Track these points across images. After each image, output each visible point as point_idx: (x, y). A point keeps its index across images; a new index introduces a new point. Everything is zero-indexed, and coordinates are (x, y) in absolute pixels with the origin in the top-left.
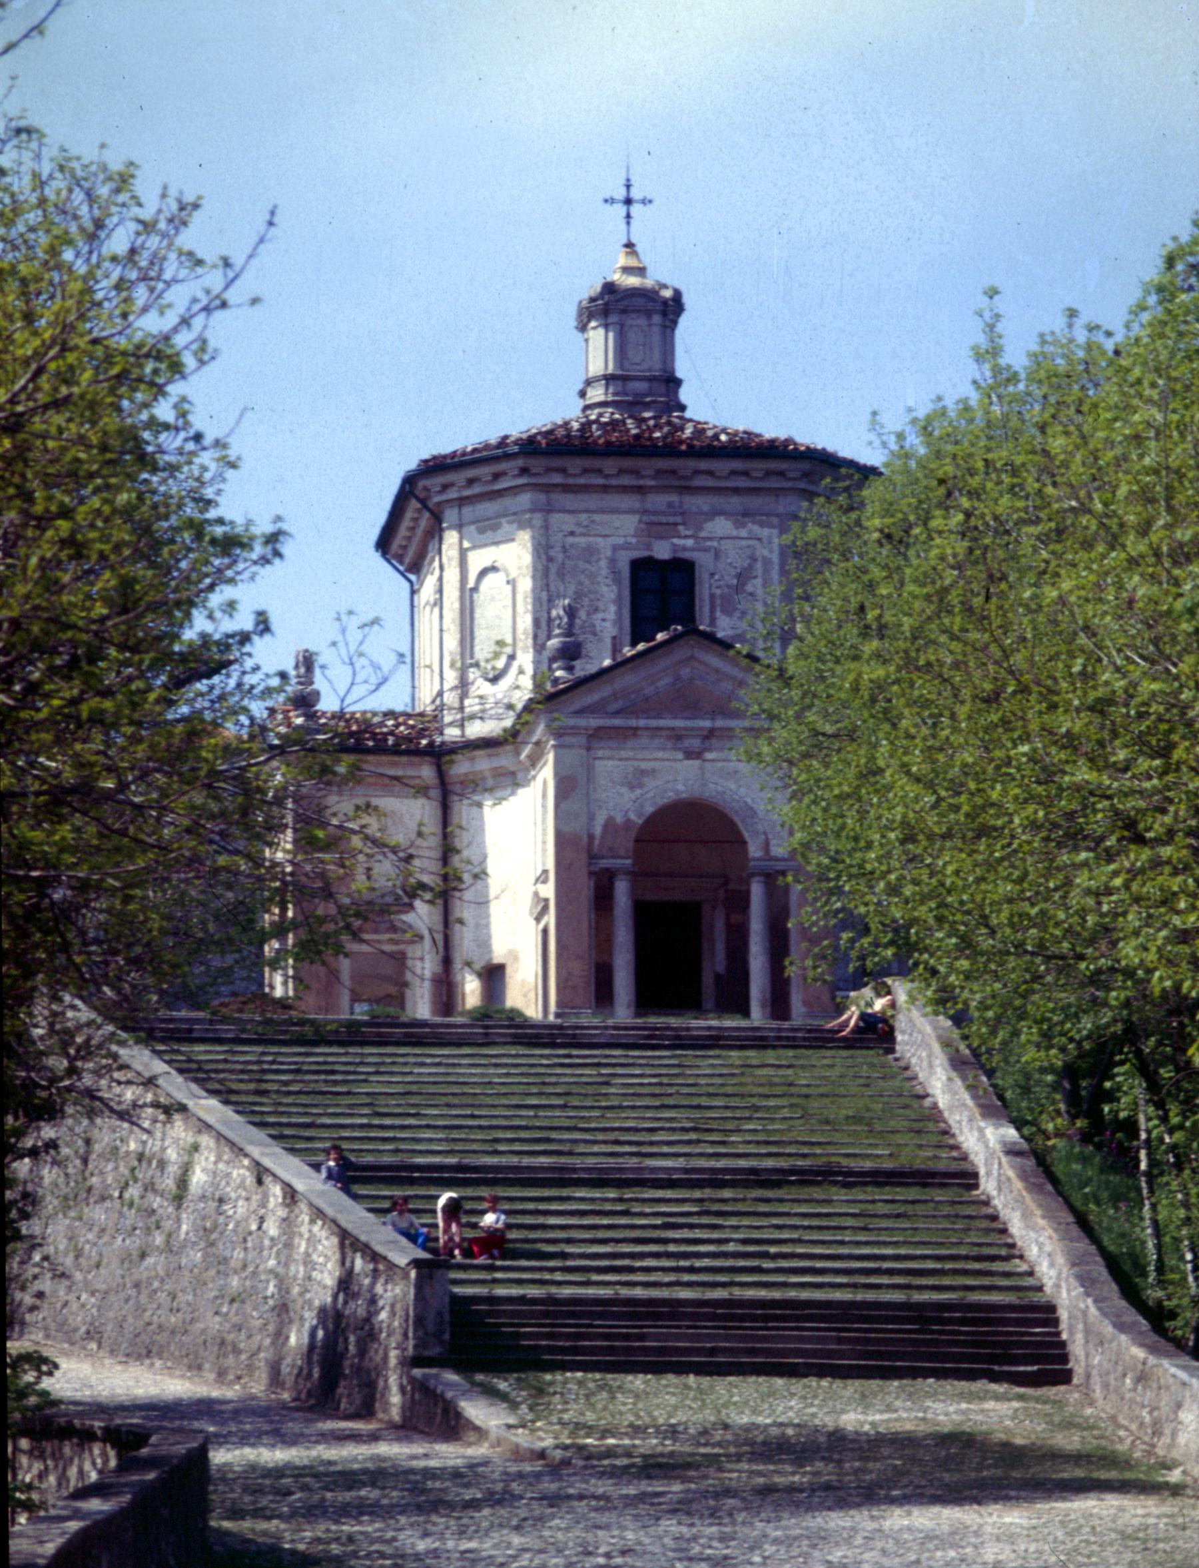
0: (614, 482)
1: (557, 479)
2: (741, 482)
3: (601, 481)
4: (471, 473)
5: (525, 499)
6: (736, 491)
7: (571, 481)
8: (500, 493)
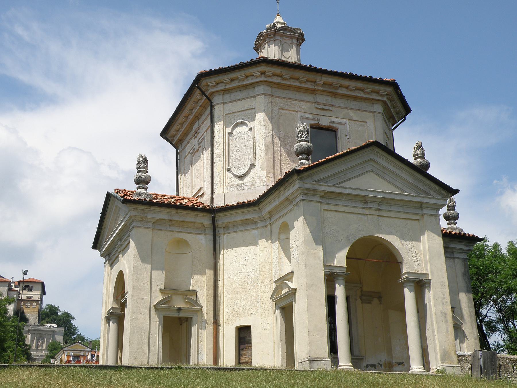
0: (303, 85)
1: (277, 80)
2: (360, 94)
3: (296, 84)
4: (233, 75)
5: (261, 89)
6: (356, 98)
7: (284, 82)
8: (246, 87)
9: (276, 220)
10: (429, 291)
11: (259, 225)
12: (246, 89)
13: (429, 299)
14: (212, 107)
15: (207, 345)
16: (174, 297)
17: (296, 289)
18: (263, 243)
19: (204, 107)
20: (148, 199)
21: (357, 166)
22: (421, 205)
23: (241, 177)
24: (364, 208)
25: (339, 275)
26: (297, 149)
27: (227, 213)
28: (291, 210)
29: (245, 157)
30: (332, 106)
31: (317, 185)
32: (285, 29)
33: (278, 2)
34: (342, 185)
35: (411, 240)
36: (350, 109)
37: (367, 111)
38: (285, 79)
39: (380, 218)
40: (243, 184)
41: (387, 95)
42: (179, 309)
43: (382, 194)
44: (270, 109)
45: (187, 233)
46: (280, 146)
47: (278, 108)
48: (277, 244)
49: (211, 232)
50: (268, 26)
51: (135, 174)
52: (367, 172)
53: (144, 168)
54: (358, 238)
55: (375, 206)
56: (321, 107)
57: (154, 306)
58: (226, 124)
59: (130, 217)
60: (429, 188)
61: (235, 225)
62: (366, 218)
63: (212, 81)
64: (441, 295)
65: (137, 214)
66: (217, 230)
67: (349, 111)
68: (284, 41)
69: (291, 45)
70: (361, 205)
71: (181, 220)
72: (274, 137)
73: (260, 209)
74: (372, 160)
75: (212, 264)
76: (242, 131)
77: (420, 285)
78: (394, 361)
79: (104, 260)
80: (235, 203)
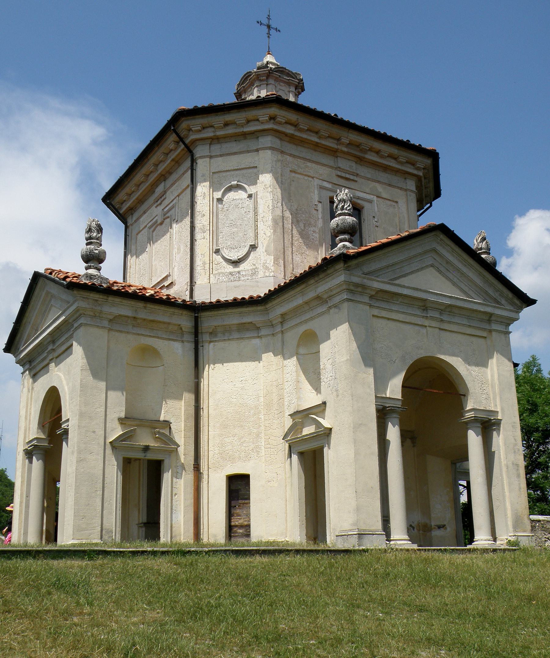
0: (323, 142)
1: (290, 130)
2: (392, 163)
3: (314, 138)
5: (267, 141)
6: (386, 169)
7: (298, 134)
8: (245, 136)
9: (292, 327)
10: (499, 435)
11: (263, 332)
12: (245, 138)
13: (499, 446)
14: (193, 161)
15: (185, 499)
16: (139, 431)
17: (331, 429)
18: (268, 357)
19: (177, 162)
20: (105, 285)
21: (415, 256)
22: (489, 318)
23: (236, 263)
24: (423, 317)
25: (393, 410)
26: (338, 225)
27: (216, 313)
28: (323, 313)
29: (241, 235)
30: (357, 175)
31: (368, 279)
32: (282, 71)
33: (269, 37)
34: (397, 282)
35: (477, 365)
36: (379, 182)
37: (398, 188)
38: (301, 130)
39: (442, 332)
40: (239, 272)
41: (424, 169)
42: (146, 449)
43: (448, 299)
44: (279, 171)
45: (158, 337)
46: (292, 223)
47: (289, 169)
48: (293, 361)
49: (191, 338)
50: (259, 64)
51: (82, 246)
52: (427, 267)
53: (97, 239)
54: (415, 358)
55: (436, 315)
56: (343, 175)
57: (111, 443)
58: (214, 187)
59: (77, 310)
60: (500, 295)
61: (227, 330)
62: (424, 331)
63: (196, 123)
64: (513, 441)
65: (87, 306)
66: (200, 336)
67: (377, 185)
68: (279, 87)
69: (287, 93)
70: (419, 313)
71: (151, 318)
72: (284, 209)
73: (267, 310)
74: (434, 250)
75: (192, 385)
76: (237, 197)
77: (488, 426)
78: (433, 524)
79: (21, 369)
80: (230, 298)
